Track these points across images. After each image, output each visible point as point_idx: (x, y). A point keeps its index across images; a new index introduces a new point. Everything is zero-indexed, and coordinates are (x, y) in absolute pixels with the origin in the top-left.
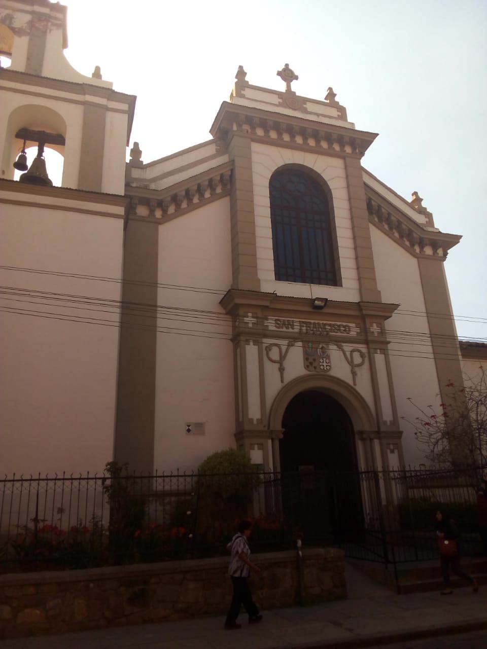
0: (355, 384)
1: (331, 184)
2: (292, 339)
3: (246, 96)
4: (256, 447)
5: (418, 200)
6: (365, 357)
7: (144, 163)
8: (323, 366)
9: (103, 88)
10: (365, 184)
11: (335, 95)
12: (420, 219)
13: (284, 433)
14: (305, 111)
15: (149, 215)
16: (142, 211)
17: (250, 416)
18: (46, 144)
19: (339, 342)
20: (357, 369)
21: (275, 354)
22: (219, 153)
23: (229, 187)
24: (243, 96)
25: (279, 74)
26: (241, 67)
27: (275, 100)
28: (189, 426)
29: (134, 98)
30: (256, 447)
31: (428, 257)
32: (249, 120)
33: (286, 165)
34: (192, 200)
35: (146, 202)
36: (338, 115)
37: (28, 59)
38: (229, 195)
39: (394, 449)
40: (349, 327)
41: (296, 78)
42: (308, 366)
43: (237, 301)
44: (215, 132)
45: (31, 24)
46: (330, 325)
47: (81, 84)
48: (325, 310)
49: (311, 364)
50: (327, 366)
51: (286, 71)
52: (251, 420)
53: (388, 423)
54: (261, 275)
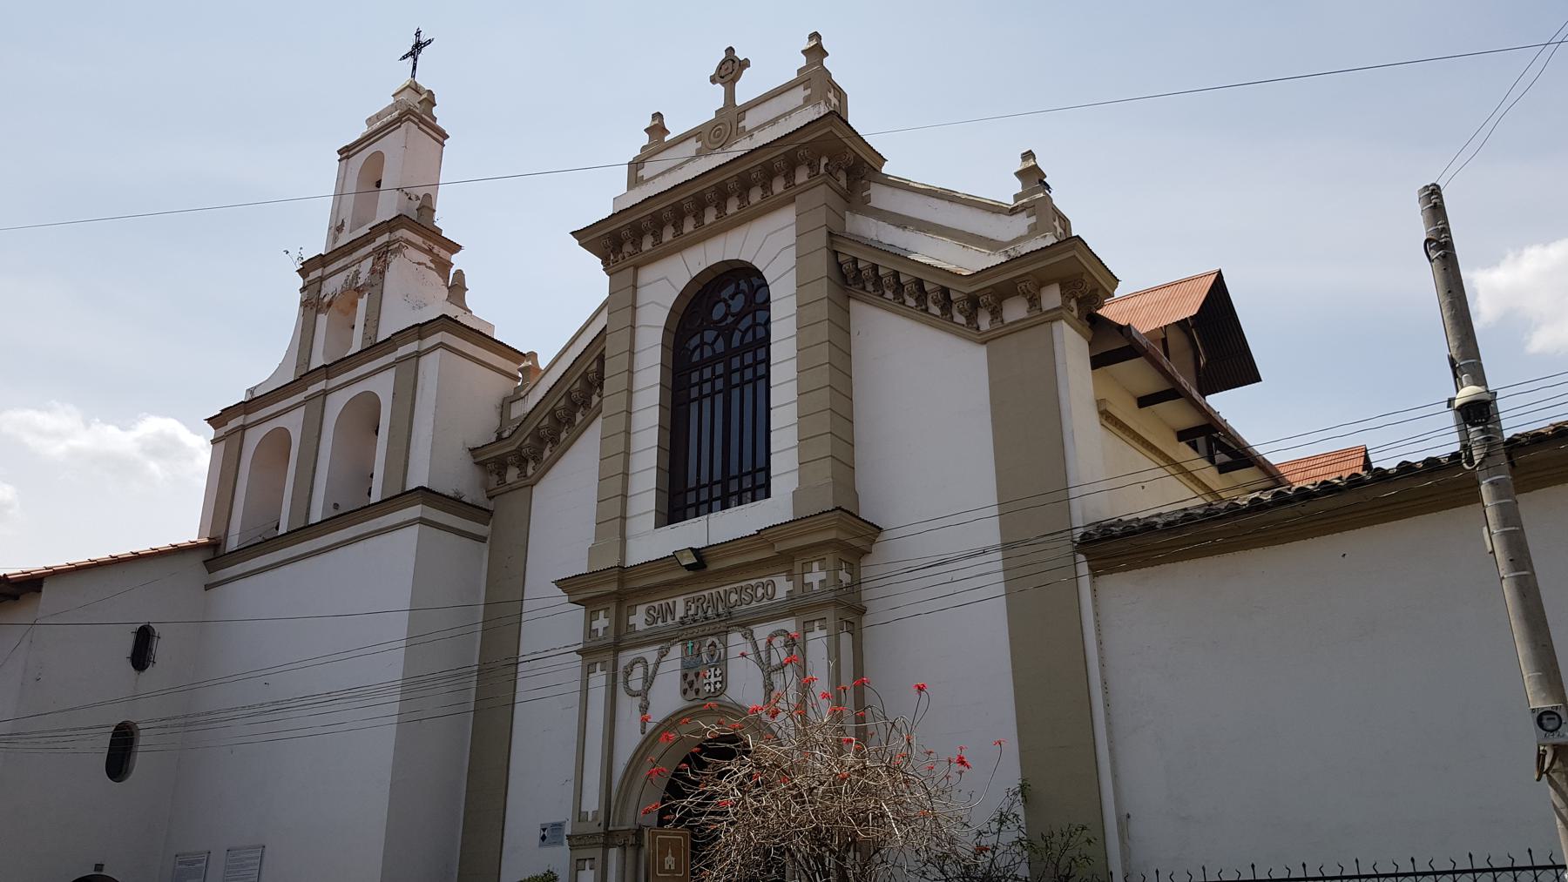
1: (769, 276)
2: (663, 640)
9: (409, 328)
16: (512, 474)
19: (745, 626)
25: (713, 80)
27: (692, 146)
28: (544, 830)
37: (365, 325)
42: (685, 692)
45: (373, 271)
46: (738, 591)
47: (389, 339)
48: (712, 567)
49: (691, 684)
50: (716, 683)
54: (633, 526)
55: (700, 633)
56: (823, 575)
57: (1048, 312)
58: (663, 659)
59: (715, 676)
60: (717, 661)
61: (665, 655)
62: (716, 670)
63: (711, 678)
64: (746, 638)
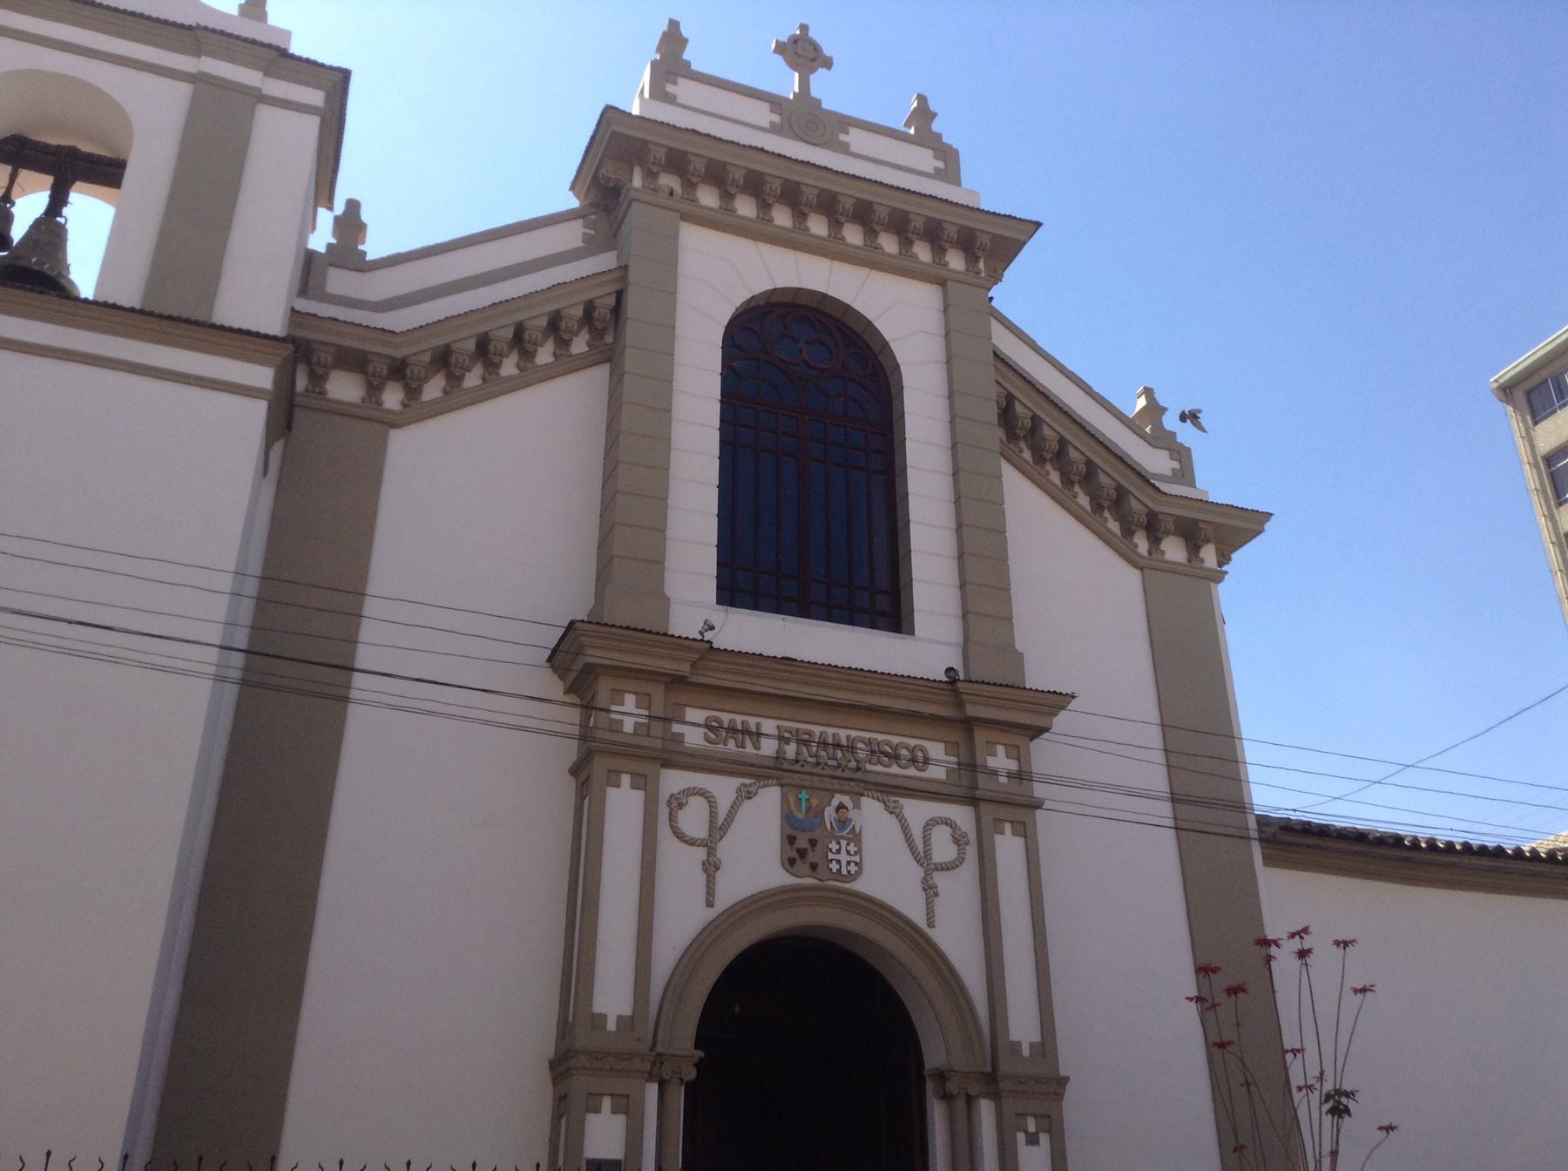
0: (931, 924)
3: (679, 100)
4: (607, 1103)
5: (1154, 410)
6: (968, 844)
7: (369, 257)
8: (839, 862)
10: (998, 356)
11: (934, 115)
12: (1155, 462)
13: (699, 1065)
14: (844, 149)
15: (363, 401)
16: (344, 388)
17: (599, 1007)
18: (78, 184)
20: (940, 879)
21: (694, 819)
22: (591, 247)
23: (609, 339)
24: (670, 99)
25: (781, 49)
26: (673, 25)
27: (762, 114)
29: (344, 76)
30: (607, 1103)
31: (1172, 569)
32: (677, 162)
33: (776, 289)
34: (497, 366)
35: (354, 361)
36: (935, 168)
38: (609, 360)
39: (1037, 1132)
40: (923, 750)
41: (828, 63)
42: (792, 862)
43: (594, 656)
44: (585, 189)
49: (802, 853)
50: (849, 863)
51: (799, 44)
52: (599, 1020)
53: (1026, 1052)
55: (818, 784)
56: (1012, 765)
57: (1168, 562)
58: (747, 803)
59: (848, 852)
60: (848, 833)
61: (750, 798)
62: (848, 844)
63: (840, 856)
64: (891, 813)
